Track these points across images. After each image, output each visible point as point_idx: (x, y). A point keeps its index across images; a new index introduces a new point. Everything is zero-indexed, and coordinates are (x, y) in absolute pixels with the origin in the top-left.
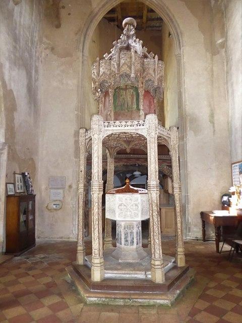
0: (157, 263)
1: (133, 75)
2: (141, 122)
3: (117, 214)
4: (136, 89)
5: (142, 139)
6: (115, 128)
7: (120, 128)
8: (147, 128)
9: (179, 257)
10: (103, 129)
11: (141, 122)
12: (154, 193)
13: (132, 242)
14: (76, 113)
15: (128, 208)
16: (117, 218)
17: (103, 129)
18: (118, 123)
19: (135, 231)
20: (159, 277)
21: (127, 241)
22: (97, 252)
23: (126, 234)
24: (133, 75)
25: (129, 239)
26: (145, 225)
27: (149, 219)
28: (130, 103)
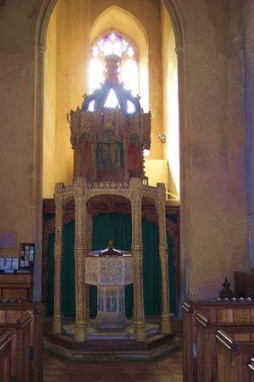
0: (139, 323)
1: (117, 133)
2: (125, 184)
3: (99, 278)
4: (121, 145)
5: (125, 204)
6: (98, 190)
7: (102, 190)
8: (131, 192)
9: (164, 323)
10: (87, 191)
11: (125, 184)
12: (138, 257)
13: (115, 309)
14: (30, 137)
15: (107, 272)
16: (97, 283)
17: (87, 191)
18: (101, 184)
19: (117, 296)
20: (141, 336)
21: (108, 306)
22: (81, 314)
23: (108, 299)
24: (117, 133)
25: (111, 305)
26: (129, 290)
27: (132, 285)
28: (113, 161)
